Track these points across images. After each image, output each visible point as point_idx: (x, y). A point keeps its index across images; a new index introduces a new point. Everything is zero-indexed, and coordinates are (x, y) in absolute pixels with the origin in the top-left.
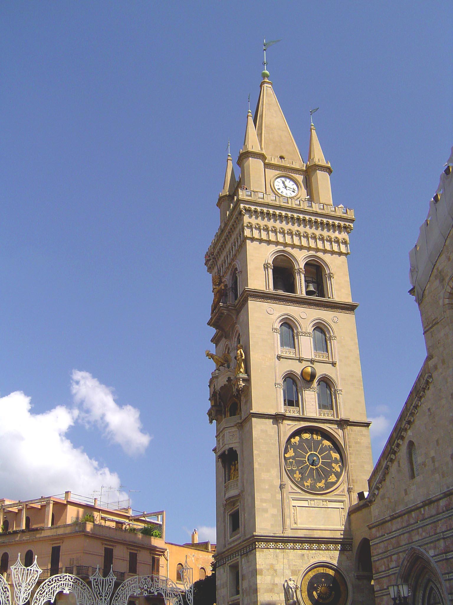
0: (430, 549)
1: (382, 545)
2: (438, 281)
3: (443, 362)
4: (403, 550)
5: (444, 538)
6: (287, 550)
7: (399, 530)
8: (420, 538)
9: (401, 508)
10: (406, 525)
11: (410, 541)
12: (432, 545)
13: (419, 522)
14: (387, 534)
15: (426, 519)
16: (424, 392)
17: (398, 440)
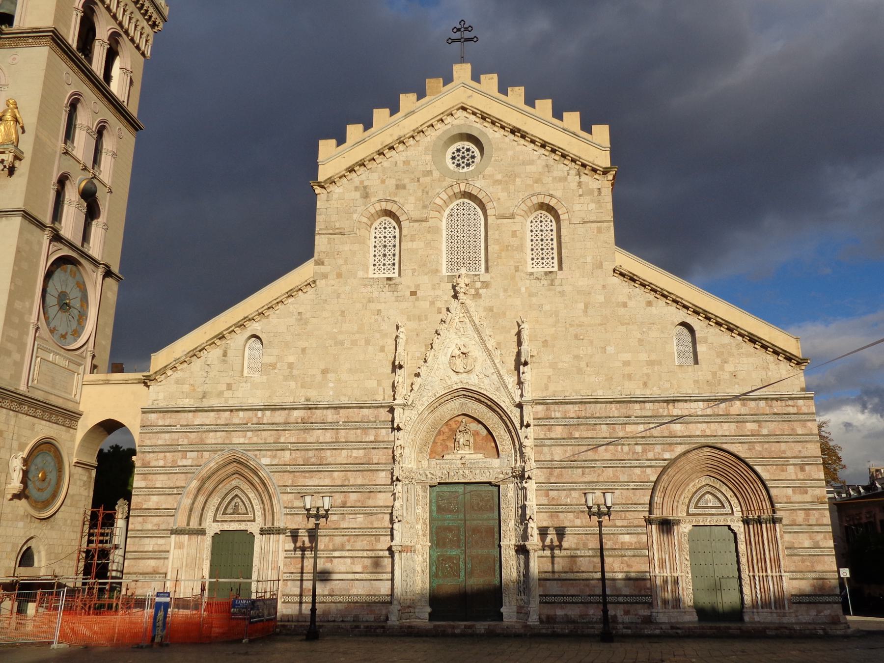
0: (264, 456)
1: (167, 436)
2: (357, 195)
3: (339, 275)
4: (211, 449)
5: (290, 450)
6: (20, 414)
7: (207, 425)
8: (246, 442)
9: (215, 402)
10: (223, 423)
11: (228, 442)
12: (269, 453)
13: (249, 424)
14: (181, 426)
15: (264, 424)
17: (236, 327)
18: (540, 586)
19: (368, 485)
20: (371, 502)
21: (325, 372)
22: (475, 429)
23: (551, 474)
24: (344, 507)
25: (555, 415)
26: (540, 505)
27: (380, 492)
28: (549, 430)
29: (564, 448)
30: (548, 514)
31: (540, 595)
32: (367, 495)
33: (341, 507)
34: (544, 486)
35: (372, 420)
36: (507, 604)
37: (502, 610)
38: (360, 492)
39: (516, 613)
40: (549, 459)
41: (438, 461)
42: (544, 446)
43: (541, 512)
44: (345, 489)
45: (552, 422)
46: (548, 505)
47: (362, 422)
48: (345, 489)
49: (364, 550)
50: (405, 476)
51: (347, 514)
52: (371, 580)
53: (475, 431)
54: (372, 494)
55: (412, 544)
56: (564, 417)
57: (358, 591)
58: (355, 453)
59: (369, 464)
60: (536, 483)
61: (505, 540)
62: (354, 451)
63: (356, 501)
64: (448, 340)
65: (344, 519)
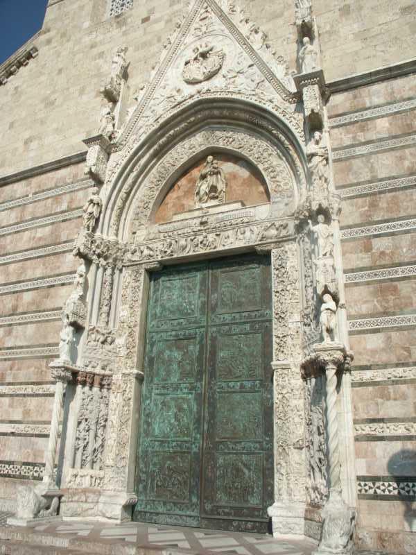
3: (63, 35)
16: (18, 67)
18: (358, 454)
19: (49, 277)
20: (49, 304)
21: (27, 142)
22: (230, 170)
23: (373, 206)
24: (12, 315)
25: (371, 103)
26: (353, 271)
27: (63, 285)
28: (363, 129)
29: (398, 154)
30: (371, 288)
31: (359, 478)
32: (44, 293)
33: (9, 316)
34: (357, 233)
35: (69, 181)
36: (285, 496)
37: (271, 511)
38: (37, 289)
39: (303, 521)
40: (368, 178)
41: (162, 228)
42: (353, 157)
43: (356, 284)
44: (19, 287)
45: (367, 114)
46: (371, 268)
47: (57, 187)
48: (19, 287)
49: (27, 383)
50: (98, 251)
51: (16, 324)
52: (32, 435)
53: (230, 174)
54: (52, 290)
55: (107, 372)
56: (389, 100)
57: (11, 455)
58: (40, 233)
59: (55, 244)
60: (342, 228)
61: (281, 356)
62: (39, 230)
63: (29, 304)
64: (182, 47)
65: (10, 333)
